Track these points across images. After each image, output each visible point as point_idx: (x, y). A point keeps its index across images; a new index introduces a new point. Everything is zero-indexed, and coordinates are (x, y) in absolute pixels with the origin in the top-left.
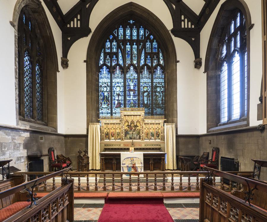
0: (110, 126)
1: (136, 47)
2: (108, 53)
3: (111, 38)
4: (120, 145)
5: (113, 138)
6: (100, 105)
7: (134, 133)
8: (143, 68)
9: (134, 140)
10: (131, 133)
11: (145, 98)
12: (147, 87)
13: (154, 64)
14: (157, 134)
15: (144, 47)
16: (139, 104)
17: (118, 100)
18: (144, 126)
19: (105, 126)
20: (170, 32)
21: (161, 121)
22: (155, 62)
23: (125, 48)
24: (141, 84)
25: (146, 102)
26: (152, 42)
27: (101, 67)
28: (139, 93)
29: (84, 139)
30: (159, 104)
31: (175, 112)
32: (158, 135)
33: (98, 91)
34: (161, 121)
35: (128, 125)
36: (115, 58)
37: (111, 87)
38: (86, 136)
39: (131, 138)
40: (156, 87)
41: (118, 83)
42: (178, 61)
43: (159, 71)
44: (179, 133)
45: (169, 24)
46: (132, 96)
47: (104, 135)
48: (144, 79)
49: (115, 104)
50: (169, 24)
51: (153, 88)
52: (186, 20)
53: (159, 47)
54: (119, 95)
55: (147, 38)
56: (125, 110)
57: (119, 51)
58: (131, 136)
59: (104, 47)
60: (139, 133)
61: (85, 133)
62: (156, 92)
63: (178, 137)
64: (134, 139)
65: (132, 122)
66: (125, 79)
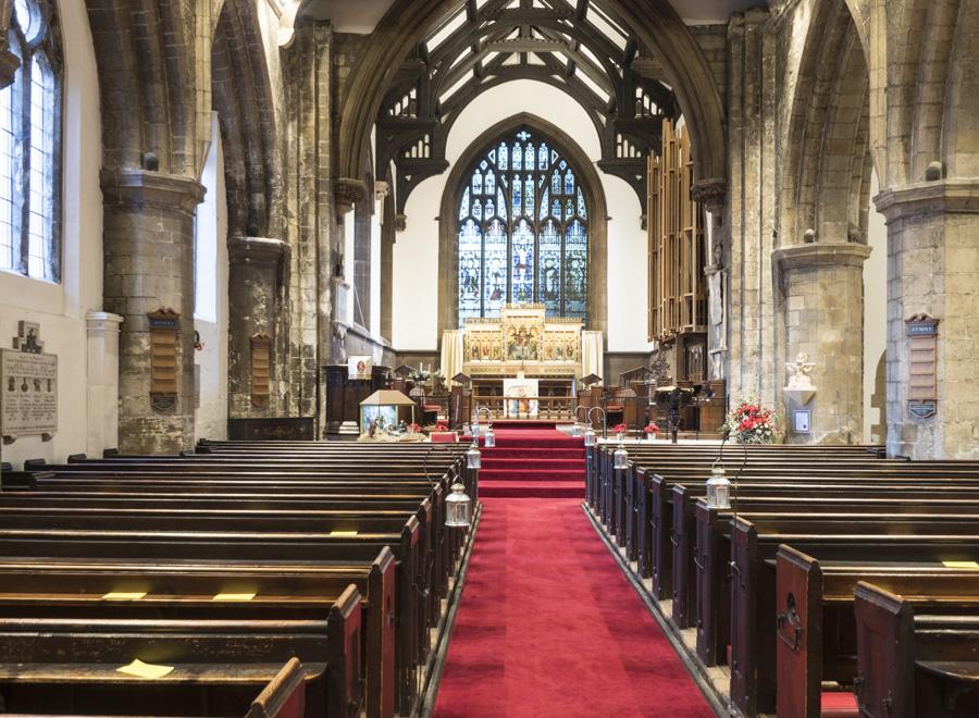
0: (481, 336)
1: (532, 183)
2: (477, 197)
3: (484, 168)
4: (499, 370)
5: (486, 357)
6: (460, 294)
7: (526, 348)
8: (544, 223)
9: (525, 362)
10: (519, 348)
11: (549, 282)
12: (553, 259)
13: (567, 217)
14: (568, 350)
15: (548, 183)
16: (536, 294)
17: (495, 285)
18: (544, 335)
19: (472, 336)
20: (595, 165)
21: (576, 327)
22: (569, 211)
23: (510, 185)
24: (541, 254)
25: (549, 289)
26: (563, 174)
27: (464, 222)
28: (536, 271)
29: (433, 358)
30: (575, 293)
31: (604, 310)
32: (570, 353)
33: (456, 268)
34: (576, 327)
35: (515, 334)
36: (490, 201)
37: (483, 260)
38: (437, 354)
39: (519, 358)
40: (571, 259)
41: (496, 252)
42: (610, 218)
43: (576, 231)
44: (611, 349)
45: (592, 149)
46: (522, 278)
47: (470, 351)
48: (548, 245)
49: (488, 292)
50: (592, 149)
51: (566, 261)
52: (626, 143)
53: (577, 183)
54: (497, 275)
55: (553, 167)
56: (510, 308)
57: (500, 190)
58: (520, 353)
59: (469, 183)
60: (535, 349)
61: (434, 347)
62: (569, 269)
63: (607, 355)
64: (526, 358)
65: (523, 329)
66: (509, 245)
